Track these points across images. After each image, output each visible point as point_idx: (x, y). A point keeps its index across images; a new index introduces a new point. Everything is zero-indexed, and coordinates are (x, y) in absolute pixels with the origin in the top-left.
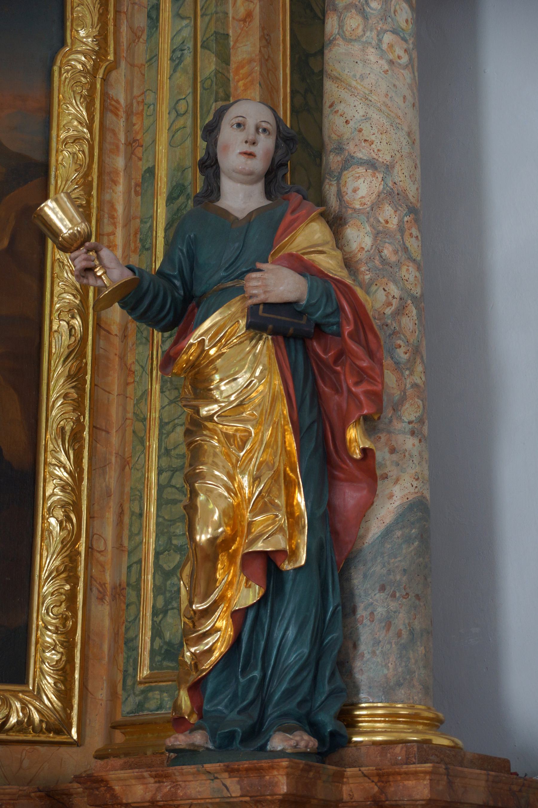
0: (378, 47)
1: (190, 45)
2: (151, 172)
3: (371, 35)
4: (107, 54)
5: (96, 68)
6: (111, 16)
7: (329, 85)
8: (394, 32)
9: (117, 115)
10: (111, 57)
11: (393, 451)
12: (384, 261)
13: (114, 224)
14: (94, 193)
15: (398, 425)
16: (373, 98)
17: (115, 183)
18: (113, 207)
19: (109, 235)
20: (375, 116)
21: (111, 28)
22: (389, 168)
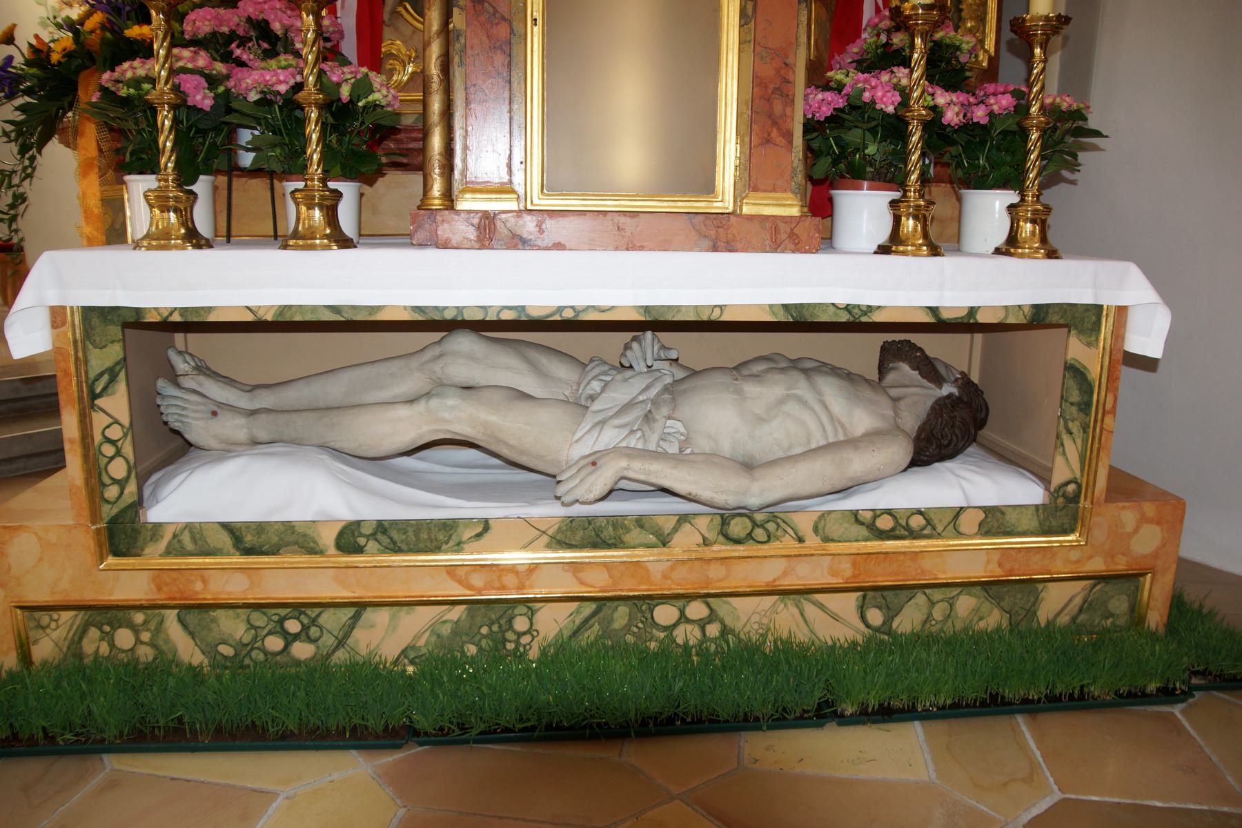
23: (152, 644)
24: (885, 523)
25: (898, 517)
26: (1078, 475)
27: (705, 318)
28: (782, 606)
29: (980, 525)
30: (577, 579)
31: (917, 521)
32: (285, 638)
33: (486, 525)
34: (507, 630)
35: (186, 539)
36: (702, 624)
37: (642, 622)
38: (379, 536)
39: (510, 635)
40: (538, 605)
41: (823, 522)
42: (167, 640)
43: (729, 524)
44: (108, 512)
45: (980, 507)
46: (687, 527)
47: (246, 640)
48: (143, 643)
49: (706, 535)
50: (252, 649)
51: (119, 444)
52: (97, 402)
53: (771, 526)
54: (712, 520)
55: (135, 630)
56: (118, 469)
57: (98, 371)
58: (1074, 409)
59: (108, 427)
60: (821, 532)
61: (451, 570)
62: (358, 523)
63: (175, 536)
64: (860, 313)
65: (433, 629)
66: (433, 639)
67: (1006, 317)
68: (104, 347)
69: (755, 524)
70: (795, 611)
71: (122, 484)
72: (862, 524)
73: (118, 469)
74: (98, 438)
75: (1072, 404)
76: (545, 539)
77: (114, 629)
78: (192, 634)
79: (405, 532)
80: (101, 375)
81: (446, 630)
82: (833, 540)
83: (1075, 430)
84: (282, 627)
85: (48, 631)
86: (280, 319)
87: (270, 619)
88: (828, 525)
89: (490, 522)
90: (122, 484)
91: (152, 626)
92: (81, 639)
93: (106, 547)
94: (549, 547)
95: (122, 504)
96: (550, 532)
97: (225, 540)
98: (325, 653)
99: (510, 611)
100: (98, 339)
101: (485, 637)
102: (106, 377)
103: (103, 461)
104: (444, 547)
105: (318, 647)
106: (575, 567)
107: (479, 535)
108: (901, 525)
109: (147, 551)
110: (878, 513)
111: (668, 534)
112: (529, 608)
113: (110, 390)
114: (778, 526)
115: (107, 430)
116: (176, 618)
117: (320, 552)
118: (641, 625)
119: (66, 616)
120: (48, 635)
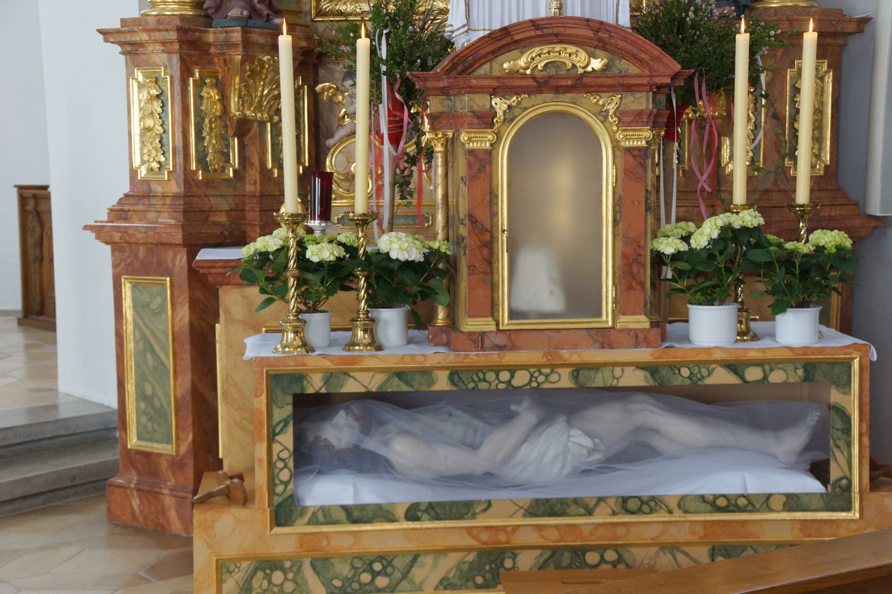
23: (294, 581)
24: (722, 503)
26: (848, 474)
27: (608, 385)
28: (662, 553)
30: (541, 535)
31: (742, 502)
32: (372, 575)
33: (489, 504)
34: (501, 567)
35: (320, 515)
36: (614, 564)
37: (578, 562)
38: (430, 511)
39: (502, 570)
40: (518, 551)
41: (683, 501)
42: (303, 578)
43: (627, 502)
44: (277, 500)
45: (783, 494)
46: (602, 504)
47: (349, 576)
48: (288, 580)
49: (614, 508)
50: (352, 582)
51: (287, 461)
52: (277, 438)
53: (652, 504)
54: (617, 500)
55: (285, 572)
58: (839, 433)
59: (281, 451)
60: (682, 507)
61: (469, 530)
62: (418, 504)
63: (314, 513)
64: (697, 379)
65: (458, 567)
66: (458, 573)
68: (283, 407)
70: (671, 557)
71: (286, 484)
73: (285, 475)
74: (275, 458)
75: (837, 429)
76: (522, 511)
77: (272, 571)
78: (318, 573)
80: (280, 422)
81: (465, 567)
82: (690, 513)
83: (841, 446)
84: (371, 568)
85: (233, 574)
86: (380, 391)
87: (364, 562)
89: (492, 502)
90: (286, 484)
91: (295, 569)
92: (252, 579)
93: (273, 523)
94: (524, 516)
95: (285, 496)
96: (525, 507)
97: (342, 515)
98: (395, 583)
99: (502, 556)
100: (279, 403)
101: (487, 571)
102: (282, 424)
103: (276, 471)
104: (466, 517)
105: (391, 580)
106: (539, 528)
109: (297, 523)
111: (592, 508)
112: (513, 553)
114: (656, 504)
115: (281, 453)
116: (310, 564)
117: (396, 521)
118: (578, 564)
119: (245, 564)
120: (232, 577)
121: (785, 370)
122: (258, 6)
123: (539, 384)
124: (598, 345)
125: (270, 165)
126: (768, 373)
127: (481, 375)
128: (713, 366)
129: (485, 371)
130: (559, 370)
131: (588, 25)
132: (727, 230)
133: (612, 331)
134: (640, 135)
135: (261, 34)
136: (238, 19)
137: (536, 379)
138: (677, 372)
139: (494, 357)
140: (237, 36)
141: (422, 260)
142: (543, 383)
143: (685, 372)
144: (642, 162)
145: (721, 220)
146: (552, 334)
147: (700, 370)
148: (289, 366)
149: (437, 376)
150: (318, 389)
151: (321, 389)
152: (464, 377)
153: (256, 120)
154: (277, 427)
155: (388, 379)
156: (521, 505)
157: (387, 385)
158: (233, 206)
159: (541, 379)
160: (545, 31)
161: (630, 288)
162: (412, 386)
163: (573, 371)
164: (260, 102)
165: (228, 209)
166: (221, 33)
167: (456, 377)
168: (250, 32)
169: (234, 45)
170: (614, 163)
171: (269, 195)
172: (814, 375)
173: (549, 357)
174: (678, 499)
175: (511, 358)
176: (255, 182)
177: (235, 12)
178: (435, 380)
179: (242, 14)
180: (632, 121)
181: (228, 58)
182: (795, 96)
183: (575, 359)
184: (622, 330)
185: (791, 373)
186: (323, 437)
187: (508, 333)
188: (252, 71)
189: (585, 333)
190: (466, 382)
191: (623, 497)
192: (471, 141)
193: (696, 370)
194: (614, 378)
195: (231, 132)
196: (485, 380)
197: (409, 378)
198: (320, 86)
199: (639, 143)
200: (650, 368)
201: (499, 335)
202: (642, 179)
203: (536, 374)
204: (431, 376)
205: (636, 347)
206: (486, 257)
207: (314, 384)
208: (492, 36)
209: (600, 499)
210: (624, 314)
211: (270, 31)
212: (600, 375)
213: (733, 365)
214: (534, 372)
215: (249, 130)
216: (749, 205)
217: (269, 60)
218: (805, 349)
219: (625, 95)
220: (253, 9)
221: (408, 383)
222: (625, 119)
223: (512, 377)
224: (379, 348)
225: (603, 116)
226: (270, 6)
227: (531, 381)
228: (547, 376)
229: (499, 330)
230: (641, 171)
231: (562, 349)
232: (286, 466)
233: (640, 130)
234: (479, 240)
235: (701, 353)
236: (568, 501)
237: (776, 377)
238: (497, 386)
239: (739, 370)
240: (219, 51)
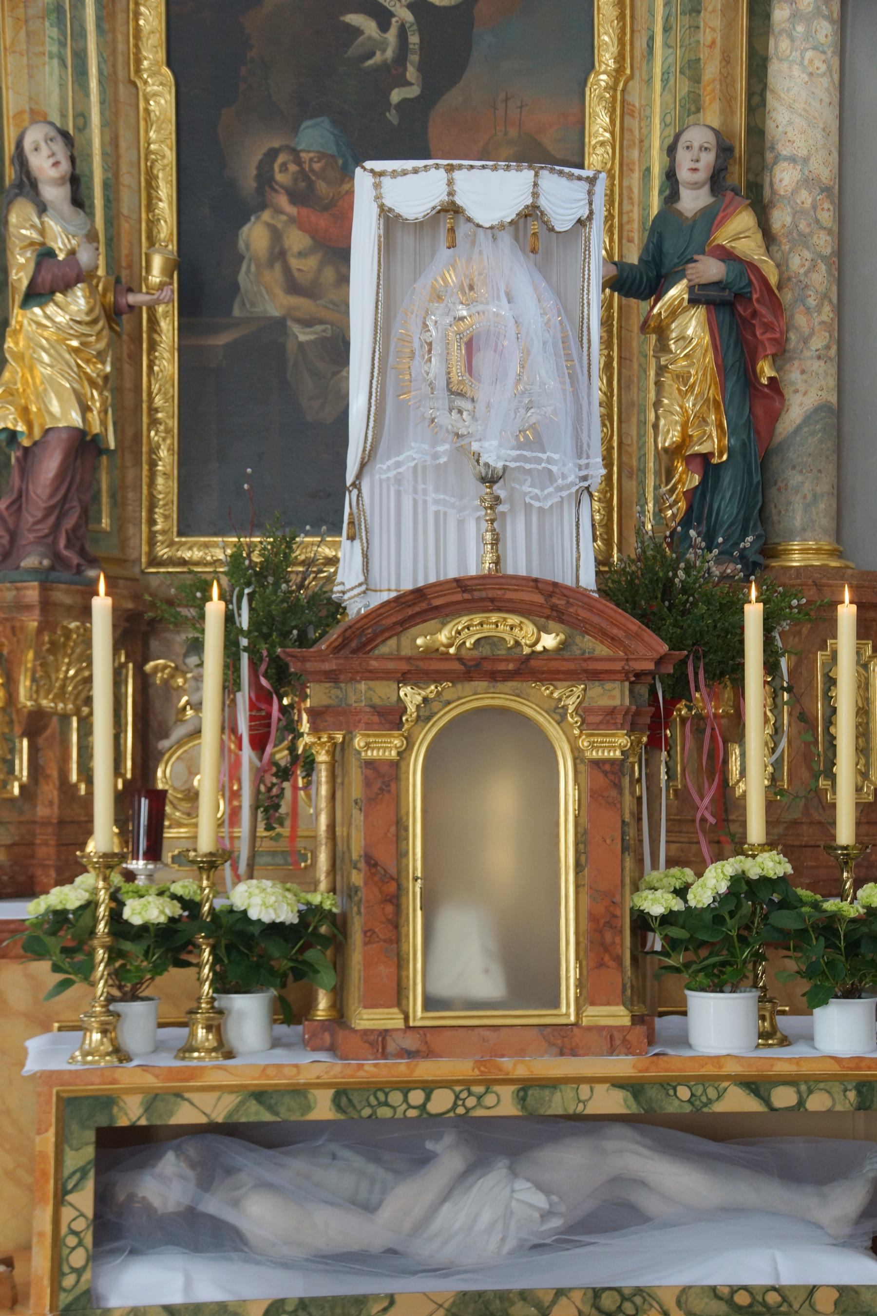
0: (801, 64)
1: (673, 69)
2: (648, 170)
3: (796, 55)
4: (625, 68)
5: (616, 83)
6: (628, 37)
7: (769, 97)
8: (814, 48)
9: (633, 116)
10: (628, 71)
11: (803, 372)
12: (801, 234)
13: (632, 204)
14: (616, 182)
15: (807, 353)
16: (796, 106)
17: (632, 171)
18: (630, 189)
19: (628, 212)
20: (797, 120)
21: (628, 48)
22: (806, 160)
25: (754, 1292)
27: (571, 1112)
29: (835, 1304)
33: (392, 1300)
41: (684, 1296)
43: (600, 1297)
44: (64, 1299)
45: (833, 1286)
46: (563, 1300)
51: (82, 1235)
52: (69, 1198)
53: (638, 1300)
54: (585, 1294)
56: (78, 1258)
57: (71, 1170)
59: (74, 1219)
60: (684, 1306)
62: (282, 1301)
67: (834, 1105)
69: (624, 1298)
71: (79, 1272)
72: (721, 1299)
73: (78, 1258)
74: (64, 1230)
79: (323, 1308)
80: (74, 1173)
86: (229, 1121)
88: (690, 1299)
89: (396, 1297)
90: (79, 1272)
95: (77, 1291)
96: (446, 1305)
102: (77, 1176)
103: (66, 1251)
107: (385, 1310)
108: (758, 1301)
110: (735, 1288)
111: (548, 1307)
113: (80, 1187)
114: (645, 1300)
115: (74, 1222)
121: (828, 1092)
122: (65, 553)
123: (468, 1110)
124: (555, 1050)
125: (74, 777)
126: (805, 1096)
127: (381, 1096)
128: (725, 1084)
129: (387, 1090)
130: (497, 1088)
131: (537, 588)
132: (739, 880)
133: (575, 1029)
134: (612, 742)
135: (67, 592)
136: (34, 572)
137: (464, 1103)
138: (671, 1092)
139: (401, 1069)
140: (32, 593)
141: (296, 921)
142: (474, 1108)
143: (684, 1093)
144: (617, 781)
145: (731, 866)
146: (486, 1033)
147: (705, 1090)
148: (92, 1084)
149: (314, 1095)
150: (134, 1119)
151: (139, 1119)
152: (356, 1098)
153: (55, 713)
154: (69, 1181)
155: (242, 1103)
156: (440, 1302)
157: (240, 1113)
158: (17, 838)
159: (471, 1102)
160: (476, 594)
161: (601, 965)
162: (277, 1114)
163: (519, 1091)
164: (63, 687)
165: (9, 842)
166: (9, 589)
167: (344, 1100)
168: (52, 589)
169: (28, 608)
170: (576, 781)
171: (73, 822)
172: (872, 1101)
173: (483, 1069)
174: (677, 1292)
175: (426, 1070)
176: (51, 803)
177: (30, 561)
178: (313, 1105)
179: (41, 563)
180: (601, 722)
181: (17, 624)
182: (830, 690)
183: (521, 1072)
184: (589, 1029)
185: (839, 1097)
186: (140, 1195)
187: (421, 1032)
188: (53, 644)
189: (535, 1032)
190: (359, 1108)
191: (594, 1289)
192: (369, 748)
193: (699, 1091)
194: (580, 1101)
195: (18, 730)
196: (386, 1104)
197: (273, 1102)
198: (152, 664)
199: (612, 754)
200: (632, 1087)
201: (409, 1033)
202: (617, 805)
203: (464, 1095)
204: (306, 1097)
205: (611, 1054)
206: (390, 917)
207: (129, 1112)
208: (403, 601)
209: (560, 1293)
210: (593, 1003)
211: (80, 587)
212: (558, 1096)
213: (753, 1083)
214: (461, 1091)
215: (45, 727)
216: (770, 844)
217: (78, 628)
218: (858, 1061)
219: (590, 684)
220: (58, 559)
221: (271, 1109)
222: (591, 719)
223: (428, 1098)
224: (229, 1055)
225: (559, 714)
226: (82, 553)
227: (455, 1105)
228: (480, 1098)
229: (408, 1027)
230: (614, 793)
231: (502, 1056)
232: (80, 1244)
233: (613, 735)
234: (381, 892)
235: (706, 1064)
236: (511, 1295)
237: (817, 1102)
238: (405, 1111)
239: (762, 1090)
240: (6, 616)
